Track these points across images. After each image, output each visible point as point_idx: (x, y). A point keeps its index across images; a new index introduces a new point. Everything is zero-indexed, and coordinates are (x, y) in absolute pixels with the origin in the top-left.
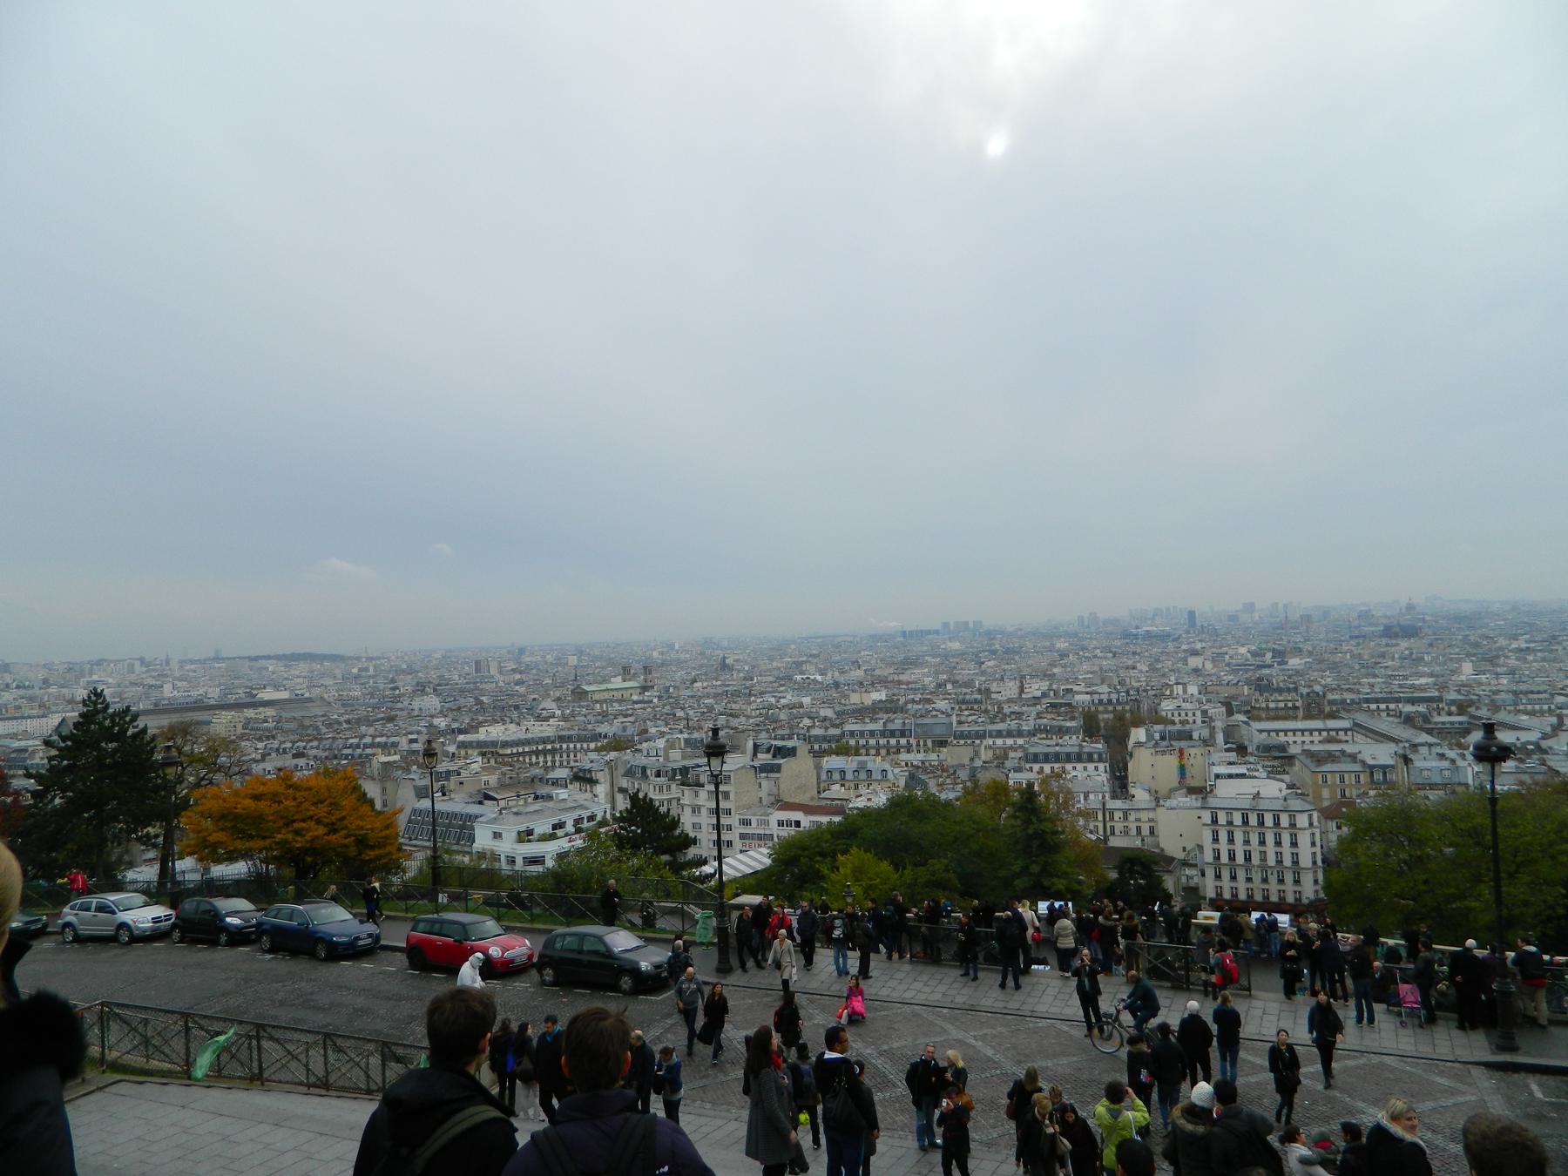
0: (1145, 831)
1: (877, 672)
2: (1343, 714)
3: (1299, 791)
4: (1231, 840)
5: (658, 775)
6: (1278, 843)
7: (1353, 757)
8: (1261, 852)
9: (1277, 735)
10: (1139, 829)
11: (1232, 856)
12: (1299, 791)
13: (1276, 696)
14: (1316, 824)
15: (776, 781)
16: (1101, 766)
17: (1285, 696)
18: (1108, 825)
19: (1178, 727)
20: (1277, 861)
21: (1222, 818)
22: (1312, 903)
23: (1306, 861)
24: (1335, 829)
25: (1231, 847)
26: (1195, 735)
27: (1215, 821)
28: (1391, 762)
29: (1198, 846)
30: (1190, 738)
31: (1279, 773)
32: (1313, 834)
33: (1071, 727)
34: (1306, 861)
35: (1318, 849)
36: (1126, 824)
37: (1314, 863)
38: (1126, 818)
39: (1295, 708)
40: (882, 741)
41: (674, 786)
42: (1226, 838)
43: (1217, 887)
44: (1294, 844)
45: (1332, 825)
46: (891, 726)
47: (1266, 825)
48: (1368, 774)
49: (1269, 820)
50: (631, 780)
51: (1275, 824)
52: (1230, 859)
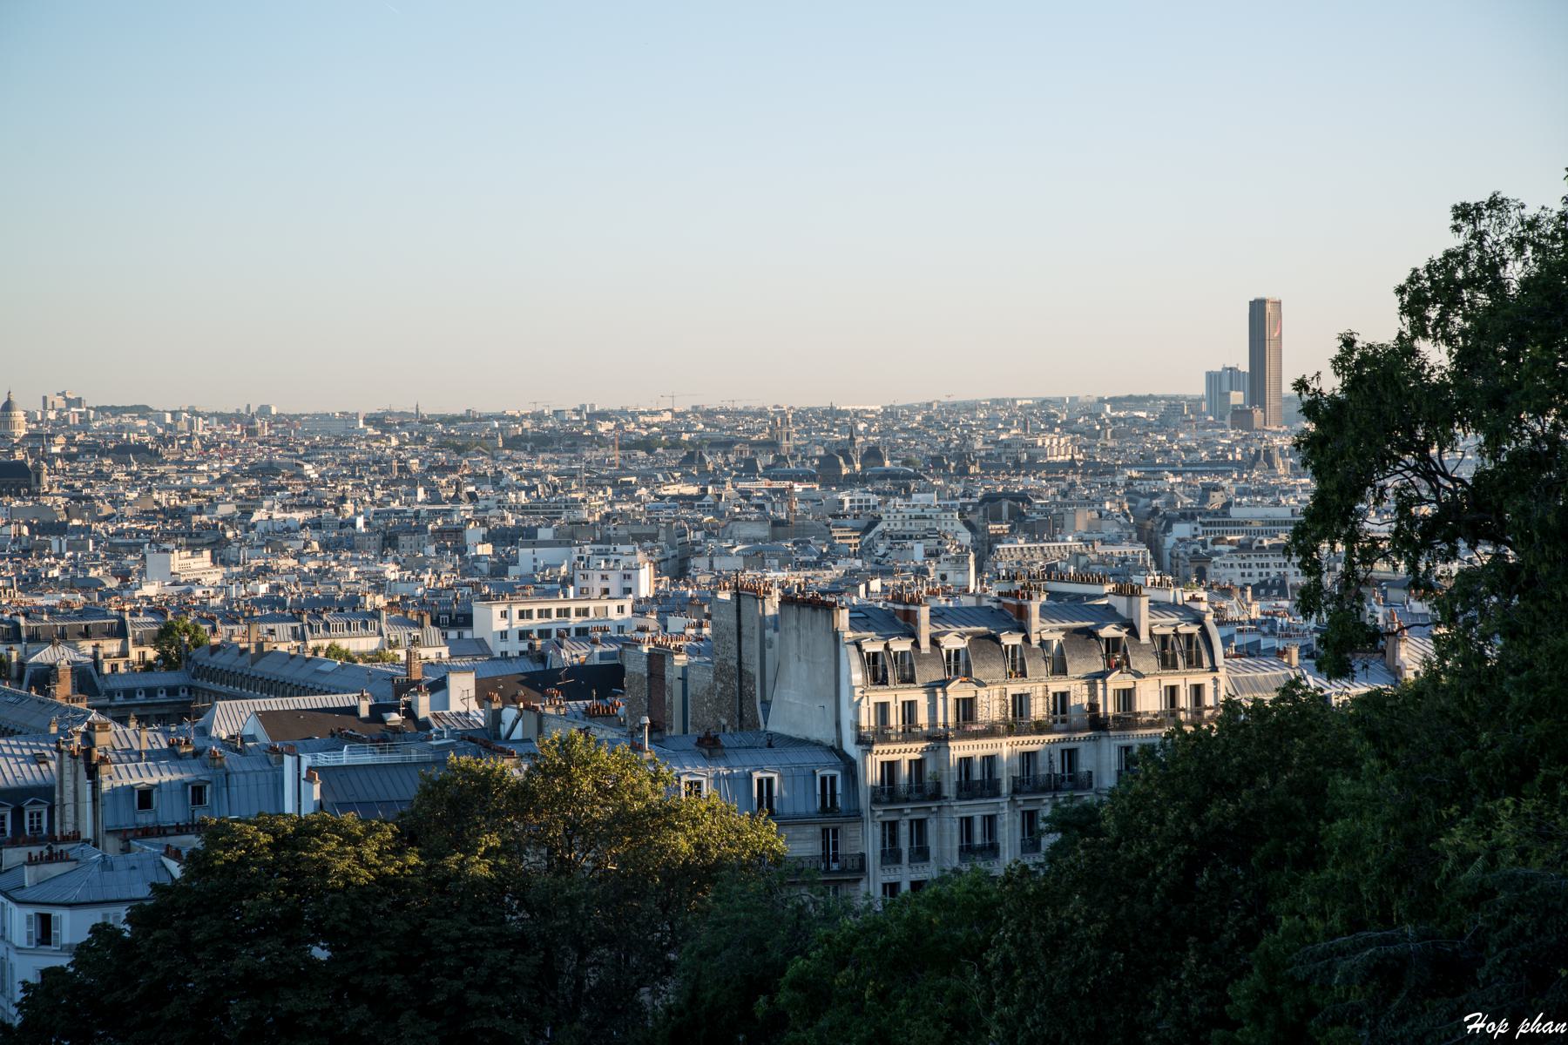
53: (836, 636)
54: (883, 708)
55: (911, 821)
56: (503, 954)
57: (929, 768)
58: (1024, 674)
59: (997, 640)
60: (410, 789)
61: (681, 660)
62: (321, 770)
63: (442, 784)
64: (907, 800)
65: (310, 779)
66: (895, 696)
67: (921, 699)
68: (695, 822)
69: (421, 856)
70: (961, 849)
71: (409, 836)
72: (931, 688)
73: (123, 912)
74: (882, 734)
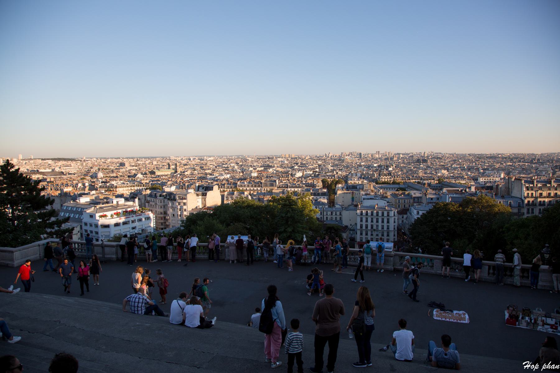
0: (338, 219)
1: (258, 169)
3: (391, 204)
4: (367, 221)
5: (160, 196)
6: (383, 222)
9: (384, 189)
10: (336, 218)
12: (391, 204)
14: (396, 215)
15: (205, 200)
16: (326, 197)
18: (325, 217)
20: (382, 228)
23: (391, 228)
24: (401, 218)
25: (367, 223)
26: (358, 187)
29: (355, 223)
30: (356, 188)
31: (385, 198)
32: (395, 219)
34: (391, 228)
35: (396, 224)
36: (332, 216)
37: (394, 229)
38: (332, 214)
39: (390, 181)
40: (252, 188)
41: (166, 200)
42: (365, 220)
43: (361, 238)
44: (388, 222)
45: (401, 216)
47: (379, 215)
48: (413, 200)
49: (380, 214)
50: (150, 198)
51: (382, 215)
52: (366, 228)
53: (522, 184)
54: (528, 194)
55: (531, 209)
56: (471, 221)
57: (535, 202)
58: (550, 190)
59: (546, 185)
60: (461, 200)
61: (500, 186)
62: (451, 197)
63: (465, 200)
64: (531, 206)
65: (450, 198)
66: (530, 192)
67: (534, 193)
68: (499, 207)
69: (462, 208)
70: (539, 213)
71: (461, 205)
72: (536, 191)
73: (426, 211)
74: (528, 197)
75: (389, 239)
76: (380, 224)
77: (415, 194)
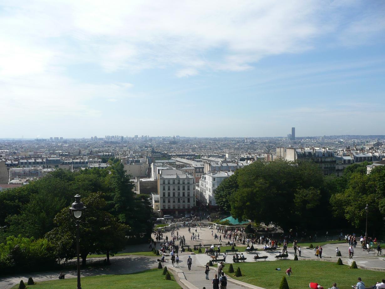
2: (172, 158)
4: (169, 189)
6: (184, 189)
7: (190, 165)
8: (178, 192)
11: (169, 195)
13: (155, 154)
14: (195, 182)
17: (157, 154)
19: (136, 159)
21: (166, 182)
22: (193, 208)
25: (169, 191)
27: (164, 183)
28: (201, 166)
32: (194, 186)
33: (99, 161)
34: (191, 195)
37: (194, 195)
43: (164, 205)
44: (189, 189)
46: (37, 161)
49: (181, 182)
75: (189, 205)
76: (181, 191)
77: (196, 165)
